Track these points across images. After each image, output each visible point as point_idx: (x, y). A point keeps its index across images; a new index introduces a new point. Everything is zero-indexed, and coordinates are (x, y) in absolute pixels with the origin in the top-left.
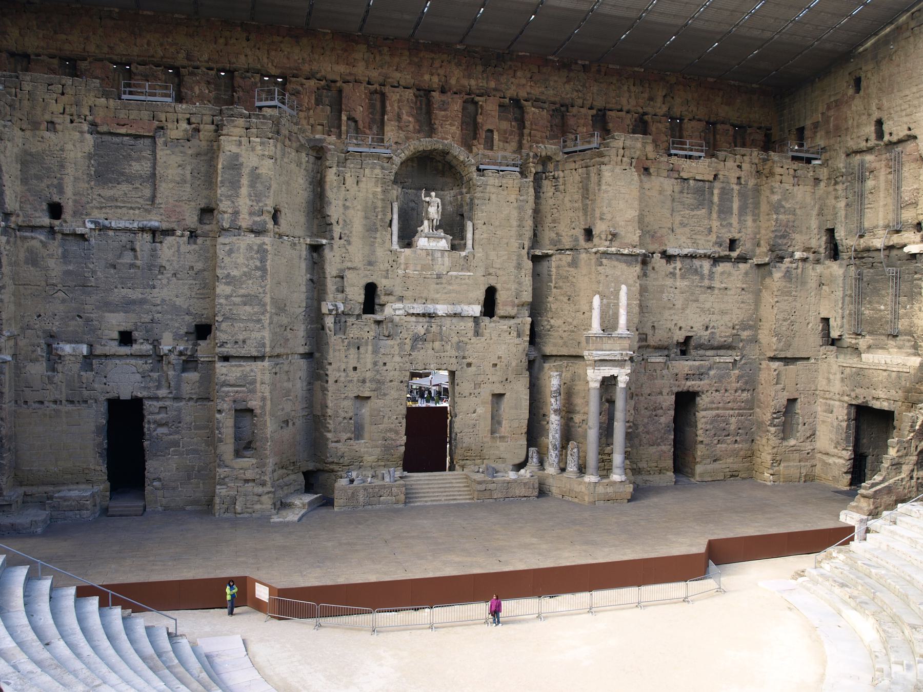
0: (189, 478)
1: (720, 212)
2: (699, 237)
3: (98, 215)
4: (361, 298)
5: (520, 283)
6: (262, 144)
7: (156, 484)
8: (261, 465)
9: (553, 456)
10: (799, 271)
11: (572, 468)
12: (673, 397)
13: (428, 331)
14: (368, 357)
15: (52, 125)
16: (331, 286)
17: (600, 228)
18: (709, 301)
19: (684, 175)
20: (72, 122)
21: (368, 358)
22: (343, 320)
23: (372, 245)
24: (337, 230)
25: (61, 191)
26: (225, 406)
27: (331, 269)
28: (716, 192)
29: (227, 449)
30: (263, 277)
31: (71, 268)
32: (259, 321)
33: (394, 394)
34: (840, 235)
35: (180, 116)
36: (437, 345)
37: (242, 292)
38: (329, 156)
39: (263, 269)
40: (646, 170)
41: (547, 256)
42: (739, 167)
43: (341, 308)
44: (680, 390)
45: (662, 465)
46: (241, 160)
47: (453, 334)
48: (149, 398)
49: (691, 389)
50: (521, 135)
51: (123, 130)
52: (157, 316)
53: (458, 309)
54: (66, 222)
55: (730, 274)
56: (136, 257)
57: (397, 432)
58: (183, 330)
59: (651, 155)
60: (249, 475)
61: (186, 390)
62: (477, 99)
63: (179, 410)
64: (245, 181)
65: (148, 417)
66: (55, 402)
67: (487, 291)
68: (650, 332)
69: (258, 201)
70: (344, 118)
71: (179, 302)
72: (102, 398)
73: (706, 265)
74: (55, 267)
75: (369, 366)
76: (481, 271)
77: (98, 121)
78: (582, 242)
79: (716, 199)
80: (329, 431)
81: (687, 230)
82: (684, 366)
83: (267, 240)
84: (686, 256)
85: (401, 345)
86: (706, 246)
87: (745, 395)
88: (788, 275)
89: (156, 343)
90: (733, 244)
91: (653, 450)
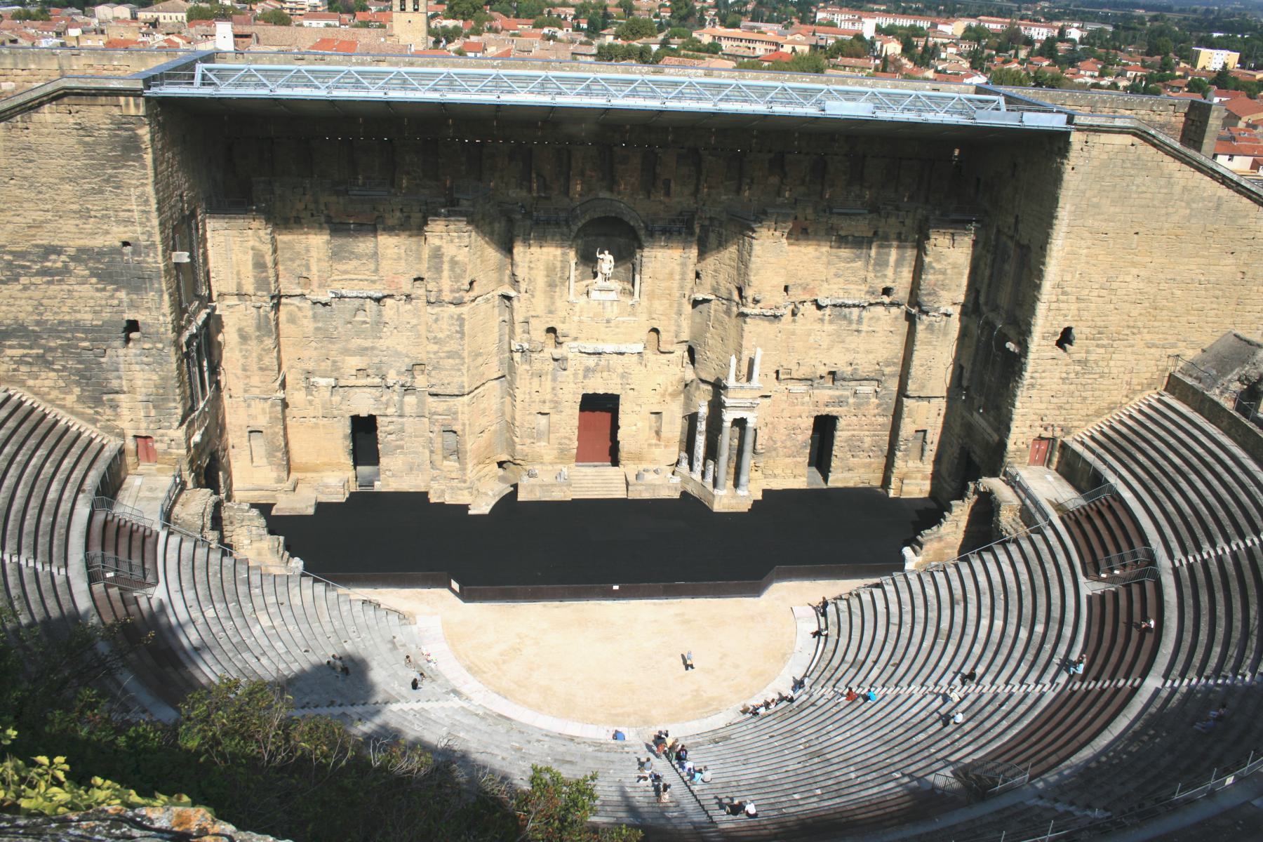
0: (411, 469)
1: (876, 264)
2: (852, 286)
3: (338, 285)
5: (679, 326)
6: (459, 237)
8: (463, 469)
9: (698, 466)
10: (943, 324)
11: (709, 479)
12: (812, 420)
13: (597, 365)
14: (548, 383)
16: (519, 329)
17: (749, 293)
18: (853, 341)
19: (842, 233)
20: (312, 215)
21: (548, 383)
23: (552, 298)
24: (523, 286)
25: (308, 269)
26: (436, 429)
27: (519, 318)
29: (438, 457)
30: (462, 339)
31: (320, 325)
32: (459, 370)
33: (568, 411)
34: (982, 299)
36: (605, 374)
37: (446, 349)
39: (462, 333)
41: (705, 301)
42: (903, 223)
43: (526, 346)
45: (796, 472)
46: (443, 250)
50: (698, 179)
52: (384, 359)
55: (879, 319)
58: (403, 369)
60: (453, 475)
61: (407, 410)
63: (403, 424)
64: (446, 266)
68: (795, 367)
69: (457, 281)
70: (534, 175)
71: (400, 348)
72: (348, 415)
73: (856, 311)
74: (309, 325)
75: (549, 390)
76: (644, 317)
77: (332, 214)
78: (736, 297)
81: (841, 280)
82: (826, 393)
83: (463, 310)
84: (835, 306)
85: (575, 375)
86: (858, 294)
87: (881, 420)
88: (930, 328)
89: (383, 378)
90: (887, 291)
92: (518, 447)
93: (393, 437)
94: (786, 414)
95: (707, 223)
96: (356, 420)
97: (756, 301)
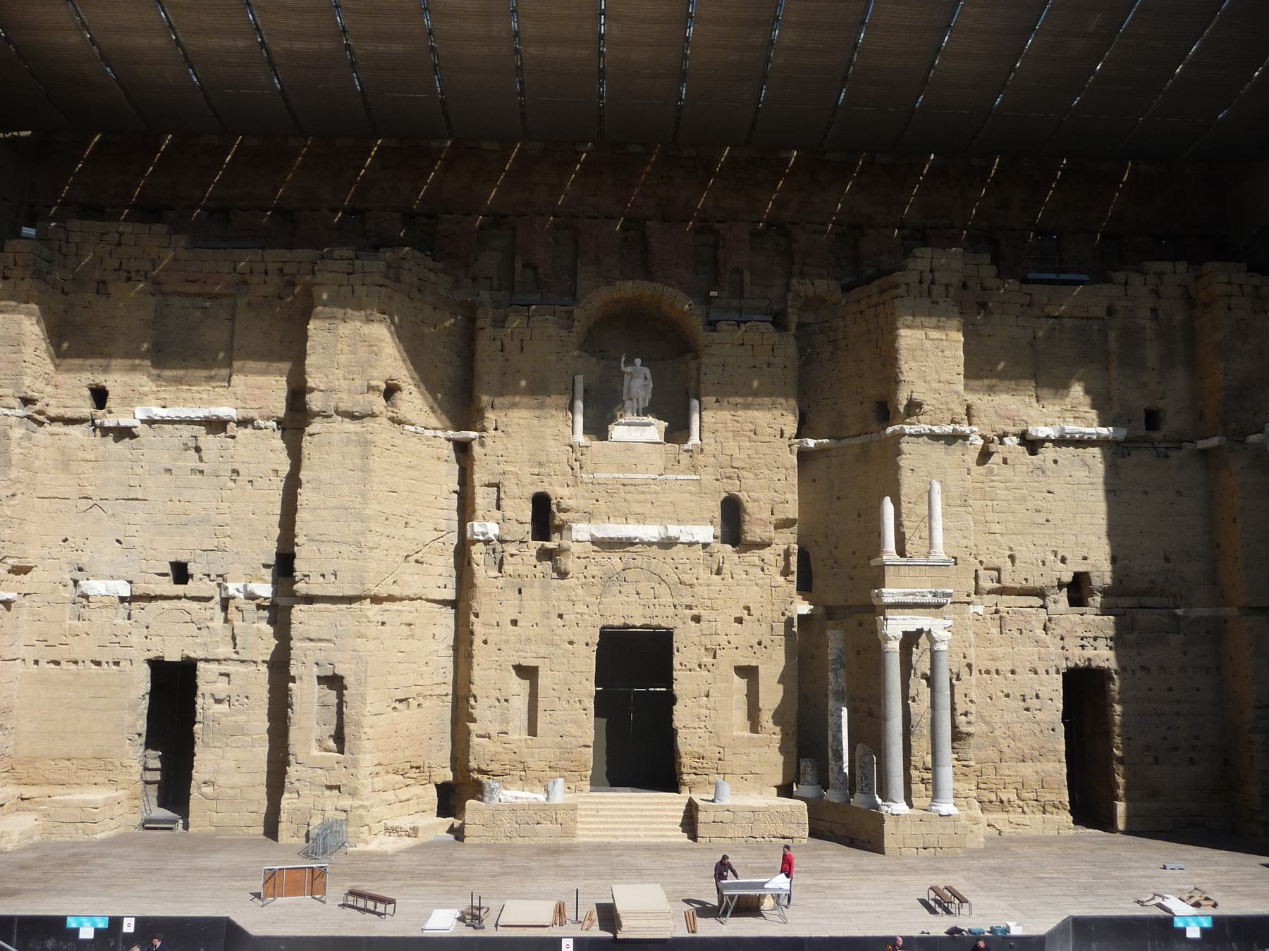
4: (527, 515)
7: (207, 790)
14: (533, 603)
15: (101, 287)
16: (483, 498)
22: (499, 548)
27: (480, 476)
28: (1113, 334)
35: (271, 266)
38: (480, 312)
40: (983, 305)
44: (1071, 665)
45: (1047, 797)
47: (670, 571)
48: (207, 660)
49: (1094, 665)
51: (192, 289)
53: (673, 531)
54: (110, 412)
56: (201, 460)
57: (577, 723)
59: (991, 282)
62: (717, 226)
65: (202, 687)
66: (76, 662)
67: (723, 503)
70: (518, 265)
79: (1113, 345)
80: (474, 721)
91: (1028, 770)
92: (475, 740)
93: (224, 707)
94: (1005, 667)
95: (810, 318)
96: (159, 667)
97: (914, 407)
